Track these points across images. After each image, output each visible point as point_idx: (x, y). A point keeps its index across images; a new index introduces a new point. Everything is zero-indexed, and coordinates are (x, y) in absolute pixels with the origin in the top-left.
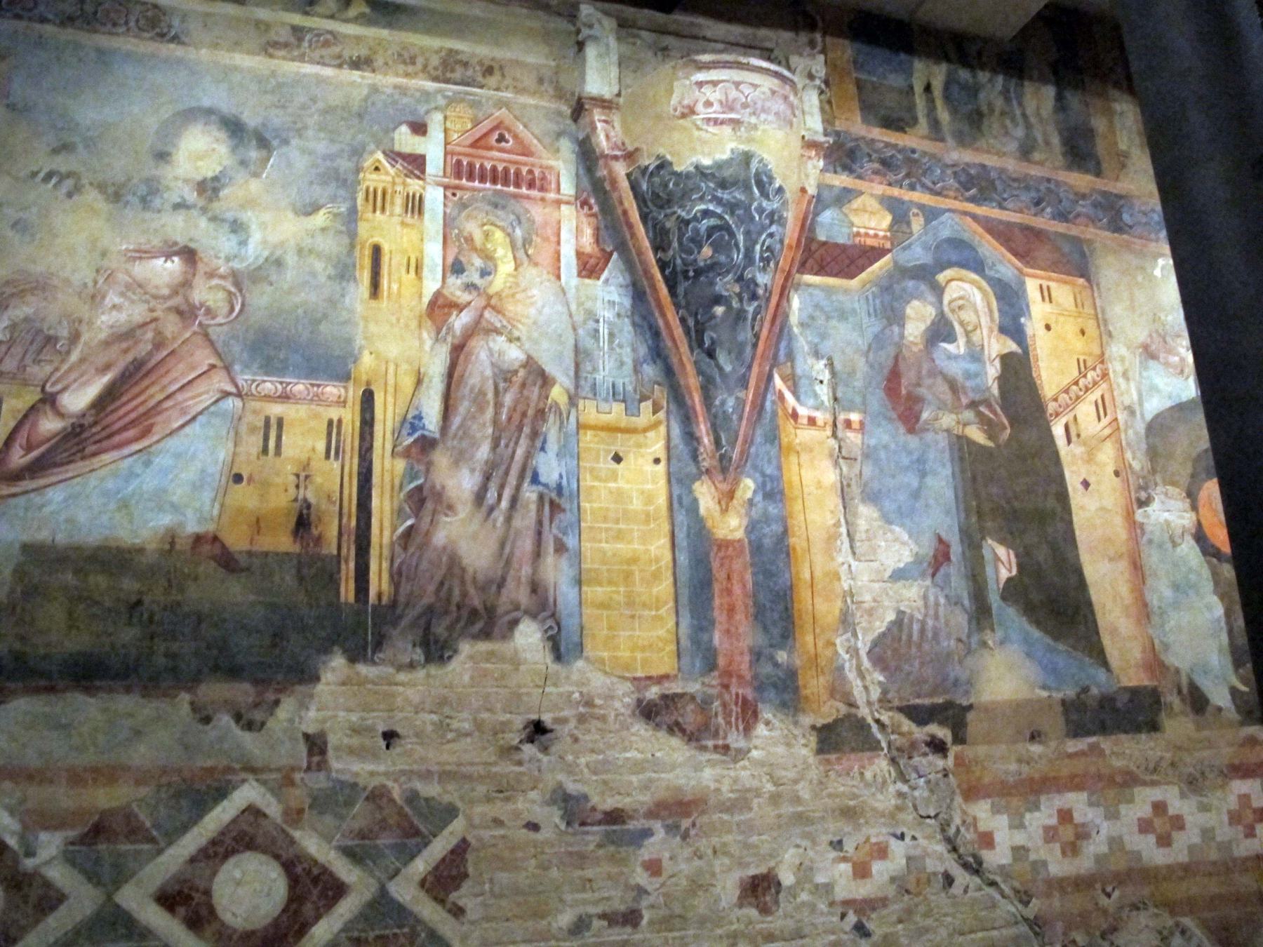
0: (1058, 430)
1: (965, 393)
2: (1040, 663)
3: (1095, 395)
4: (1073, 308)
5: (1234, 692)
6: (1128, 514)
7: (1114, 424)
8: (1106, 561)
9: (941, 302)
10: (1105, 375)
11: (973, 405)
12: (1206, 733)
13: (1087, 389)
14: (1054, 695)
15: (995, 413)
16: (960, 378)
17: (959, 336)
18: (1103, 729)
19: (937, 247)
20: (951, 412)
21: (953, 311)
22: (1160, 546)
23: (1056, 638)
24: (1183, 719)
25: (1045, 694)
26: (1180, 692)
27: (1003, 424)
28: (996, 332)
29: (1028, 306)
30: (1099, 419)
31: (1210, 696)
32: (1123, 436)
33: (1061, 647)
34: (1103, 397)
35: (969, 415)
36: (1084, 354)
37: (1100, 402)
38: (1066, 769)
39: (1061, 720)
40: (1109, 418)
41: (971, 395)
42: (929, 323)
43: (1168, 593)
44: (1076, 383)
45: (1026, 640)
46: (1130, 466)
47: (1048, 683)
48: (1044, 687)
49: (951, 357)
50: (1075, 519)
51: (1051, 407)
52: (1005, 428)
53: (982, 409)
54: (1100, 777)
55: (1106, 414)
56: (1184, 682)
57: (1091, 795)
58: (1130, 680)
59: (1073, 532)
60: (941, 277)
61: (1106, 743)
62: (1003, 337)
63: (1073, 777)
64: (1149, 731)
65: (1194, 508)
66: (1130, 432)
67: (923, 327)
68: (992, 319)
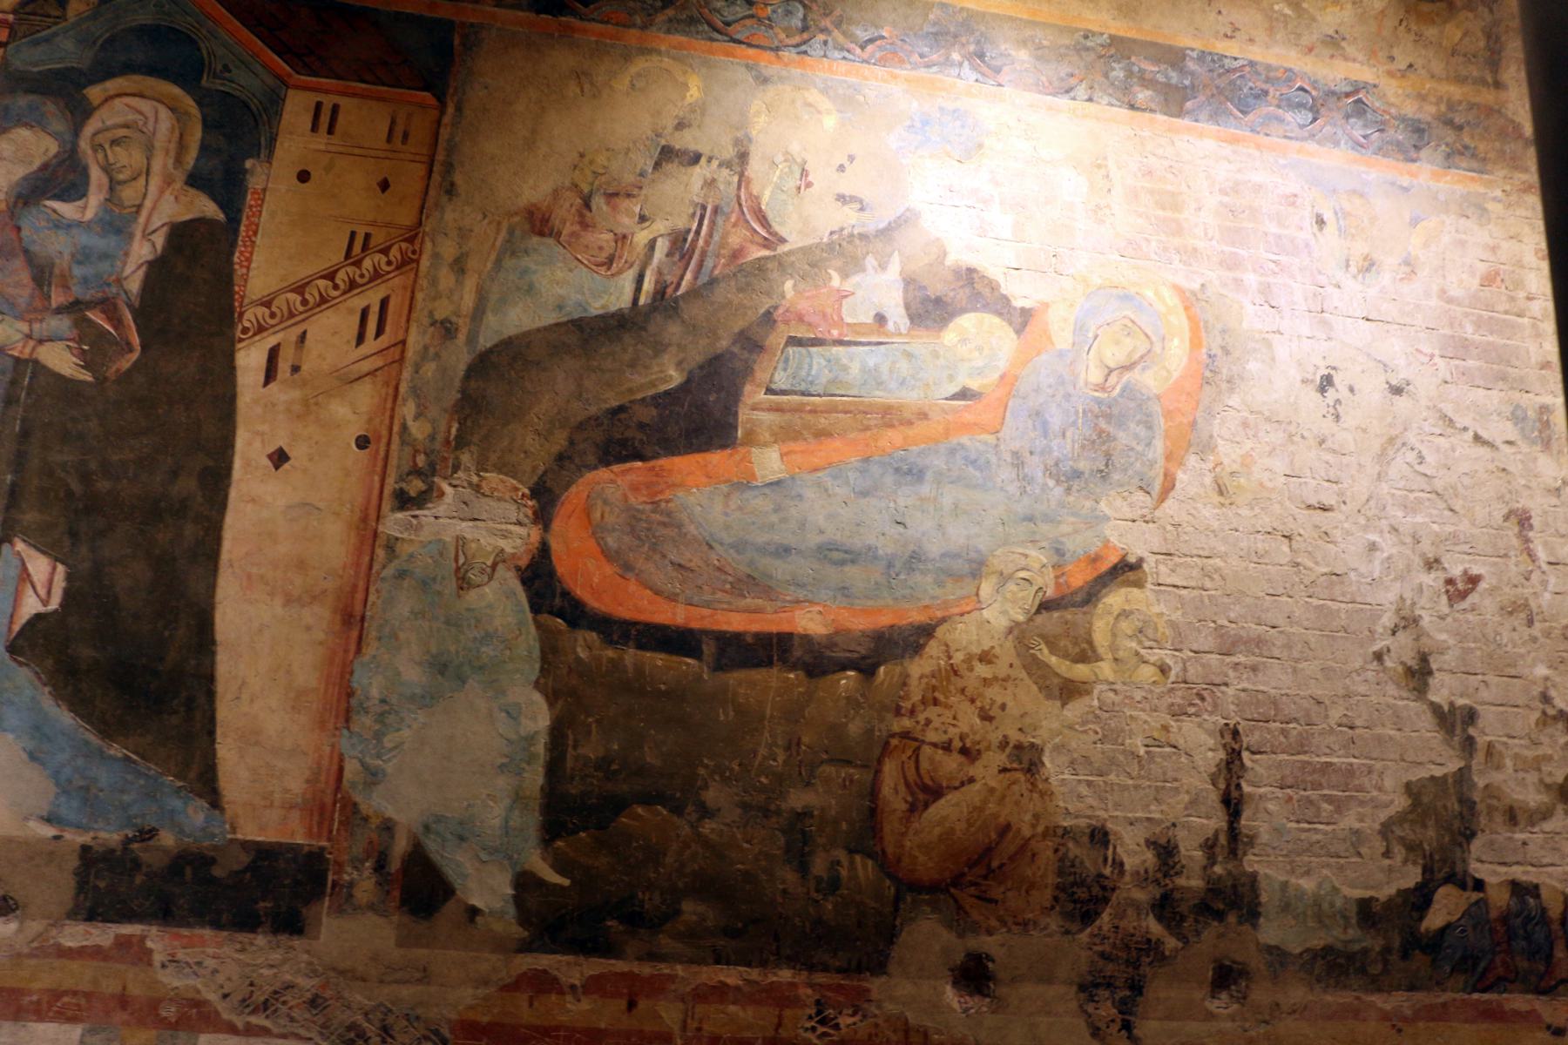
0: (250, 359)
1: (66, 287)
2: (56, 775)
3: (373, 298)
4: (382, 144)
5: (525, 883)
6: (364, 519)
7: (397, 351)
8: (278, 601)
9: (77, 132)
10: (408, 263)
11: (75, 308)
12: (420, 953)
13: (352, 285)
14: (68, 836)
15: (118, 322)
16: (63, 263)
17: (93, 188)
18: (165, 913)
19: (111, 41)
20: (20, 318)
21: (98, 147)
22: (425, 584)
23: (107, 729)
24: (372, 919)
25: (49, 831)
26: (380, 867)
27: (129, 344)
28: (178, 185)
29: (273, 140)
30: (361, 339)
31: (457, 883)
32: (406, 374)
33: (116, 750)
34: (384, 303)
35: (62, 324)
36: (373, 224)
37: (375, 309)
38: (46, 977)
39: (68, 884)
40: (385, 340)
41: (77, 291)
42: (37, 164)
43: (413, 675)
44: (331, 276)
45: (39, 730)
46: (404, 427)
47: (64, 812)
48: (49, 820)
49: (60, 224)
50: (229, 519)
51: (250, 316)
52: (131, 350)
53: (95, 316)
54: (123, 1001)
55: (380, 331)
56: (401, 846)
57: (92, 1031)
58: (262, 829)
59: (218, 540)
60: (94, 93)
61: (157, 939)
62: (192, 191)
63: (57, 995)
64: (276, 931)
65: (543, 517)
66: (430, 369)
67: (20, 172)
68: (178, 161)
